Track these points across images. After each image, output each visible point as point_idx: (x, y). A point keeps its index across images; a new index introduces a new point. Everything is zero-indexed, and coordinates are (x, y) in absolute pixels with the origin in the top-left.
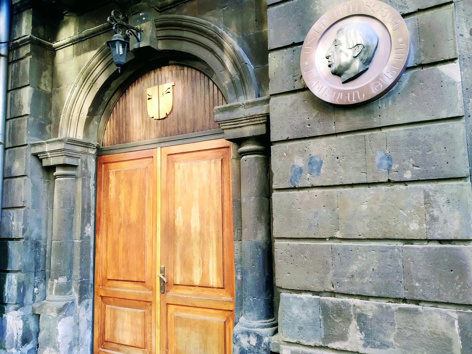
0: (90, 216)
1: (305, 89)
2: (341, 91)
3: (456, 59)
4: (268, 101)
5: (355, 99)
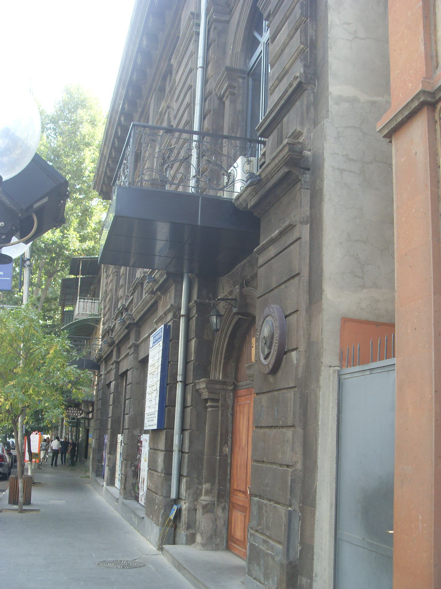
0: (228, 439)
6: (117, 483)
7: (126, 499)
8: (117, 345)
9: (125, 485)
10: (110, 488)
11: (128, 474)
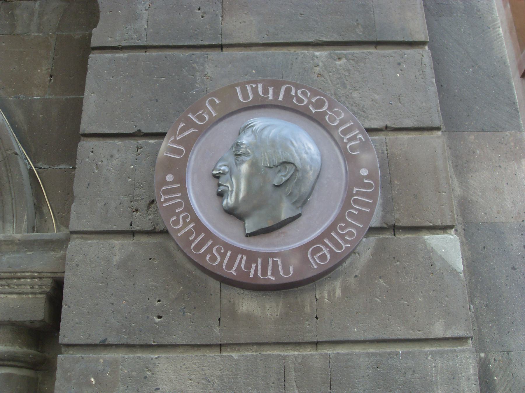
1: (165, 232)
2: (243, 252)
3: (451, 227)
4: (61, 244)
5: (272, 275)
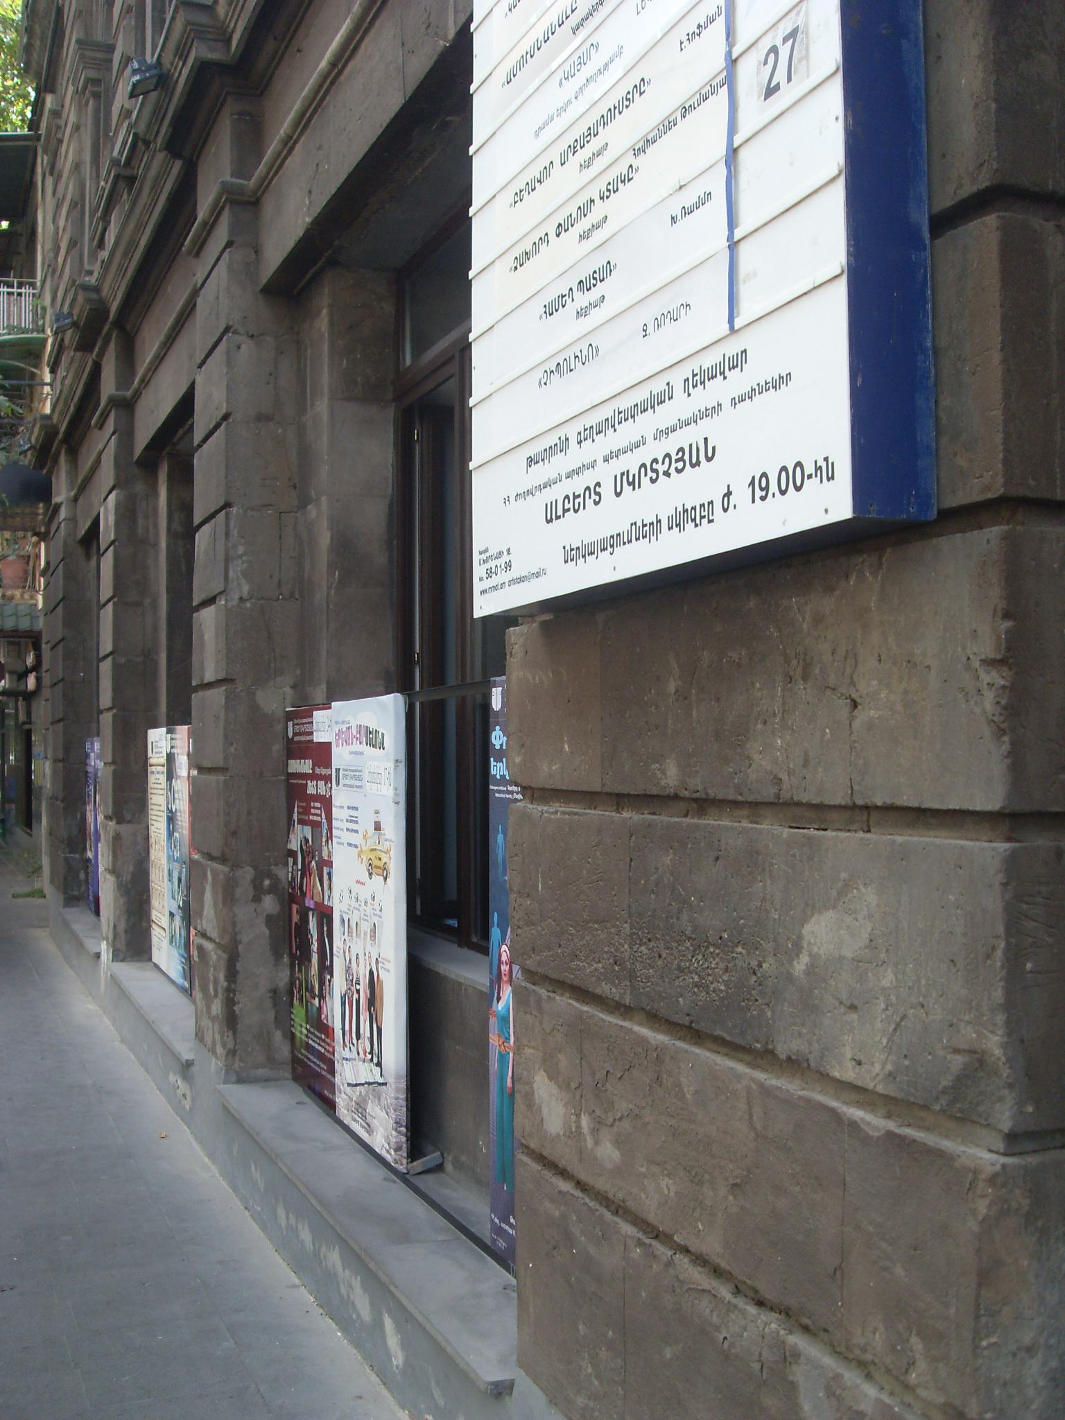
6: (166, 953)
7: (241, 1080)
8: (120, 323)
9: (230, 1003)
10: (128, 972)
11: (245, 938)
